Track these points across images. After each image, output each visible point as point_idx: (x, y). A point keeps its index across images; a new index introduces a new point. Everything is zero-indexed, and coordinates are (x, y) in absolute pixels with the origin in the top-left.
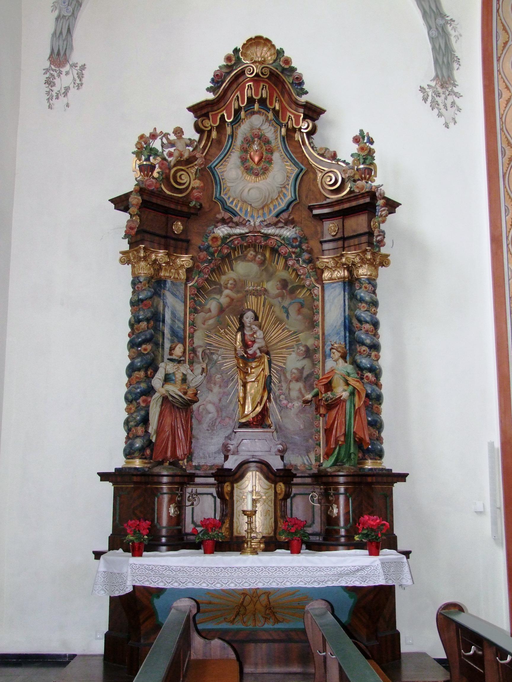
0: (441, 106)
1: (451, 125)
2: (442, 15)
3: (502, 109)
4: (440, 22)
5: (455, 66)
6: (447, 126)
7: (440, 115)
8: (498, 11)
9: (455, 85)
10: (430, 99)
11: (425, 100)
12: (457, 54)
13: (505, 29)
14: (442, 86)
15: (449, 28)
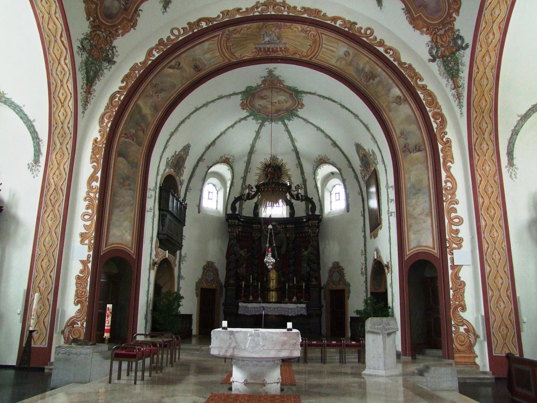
0: (34, 170)
1: (36, 177)
2: (39, 139)
3: (49, 171)
4: (38, 141)
5: (41, 156)
6: (34, 178)
7: (33, 173)
8: (53, 138)
9: (39, 163)
10: (30, 168)
11: (29, 168)
12: (42, 152)
13: (55, 144)
14: (35, 163)
15: (40, 142)
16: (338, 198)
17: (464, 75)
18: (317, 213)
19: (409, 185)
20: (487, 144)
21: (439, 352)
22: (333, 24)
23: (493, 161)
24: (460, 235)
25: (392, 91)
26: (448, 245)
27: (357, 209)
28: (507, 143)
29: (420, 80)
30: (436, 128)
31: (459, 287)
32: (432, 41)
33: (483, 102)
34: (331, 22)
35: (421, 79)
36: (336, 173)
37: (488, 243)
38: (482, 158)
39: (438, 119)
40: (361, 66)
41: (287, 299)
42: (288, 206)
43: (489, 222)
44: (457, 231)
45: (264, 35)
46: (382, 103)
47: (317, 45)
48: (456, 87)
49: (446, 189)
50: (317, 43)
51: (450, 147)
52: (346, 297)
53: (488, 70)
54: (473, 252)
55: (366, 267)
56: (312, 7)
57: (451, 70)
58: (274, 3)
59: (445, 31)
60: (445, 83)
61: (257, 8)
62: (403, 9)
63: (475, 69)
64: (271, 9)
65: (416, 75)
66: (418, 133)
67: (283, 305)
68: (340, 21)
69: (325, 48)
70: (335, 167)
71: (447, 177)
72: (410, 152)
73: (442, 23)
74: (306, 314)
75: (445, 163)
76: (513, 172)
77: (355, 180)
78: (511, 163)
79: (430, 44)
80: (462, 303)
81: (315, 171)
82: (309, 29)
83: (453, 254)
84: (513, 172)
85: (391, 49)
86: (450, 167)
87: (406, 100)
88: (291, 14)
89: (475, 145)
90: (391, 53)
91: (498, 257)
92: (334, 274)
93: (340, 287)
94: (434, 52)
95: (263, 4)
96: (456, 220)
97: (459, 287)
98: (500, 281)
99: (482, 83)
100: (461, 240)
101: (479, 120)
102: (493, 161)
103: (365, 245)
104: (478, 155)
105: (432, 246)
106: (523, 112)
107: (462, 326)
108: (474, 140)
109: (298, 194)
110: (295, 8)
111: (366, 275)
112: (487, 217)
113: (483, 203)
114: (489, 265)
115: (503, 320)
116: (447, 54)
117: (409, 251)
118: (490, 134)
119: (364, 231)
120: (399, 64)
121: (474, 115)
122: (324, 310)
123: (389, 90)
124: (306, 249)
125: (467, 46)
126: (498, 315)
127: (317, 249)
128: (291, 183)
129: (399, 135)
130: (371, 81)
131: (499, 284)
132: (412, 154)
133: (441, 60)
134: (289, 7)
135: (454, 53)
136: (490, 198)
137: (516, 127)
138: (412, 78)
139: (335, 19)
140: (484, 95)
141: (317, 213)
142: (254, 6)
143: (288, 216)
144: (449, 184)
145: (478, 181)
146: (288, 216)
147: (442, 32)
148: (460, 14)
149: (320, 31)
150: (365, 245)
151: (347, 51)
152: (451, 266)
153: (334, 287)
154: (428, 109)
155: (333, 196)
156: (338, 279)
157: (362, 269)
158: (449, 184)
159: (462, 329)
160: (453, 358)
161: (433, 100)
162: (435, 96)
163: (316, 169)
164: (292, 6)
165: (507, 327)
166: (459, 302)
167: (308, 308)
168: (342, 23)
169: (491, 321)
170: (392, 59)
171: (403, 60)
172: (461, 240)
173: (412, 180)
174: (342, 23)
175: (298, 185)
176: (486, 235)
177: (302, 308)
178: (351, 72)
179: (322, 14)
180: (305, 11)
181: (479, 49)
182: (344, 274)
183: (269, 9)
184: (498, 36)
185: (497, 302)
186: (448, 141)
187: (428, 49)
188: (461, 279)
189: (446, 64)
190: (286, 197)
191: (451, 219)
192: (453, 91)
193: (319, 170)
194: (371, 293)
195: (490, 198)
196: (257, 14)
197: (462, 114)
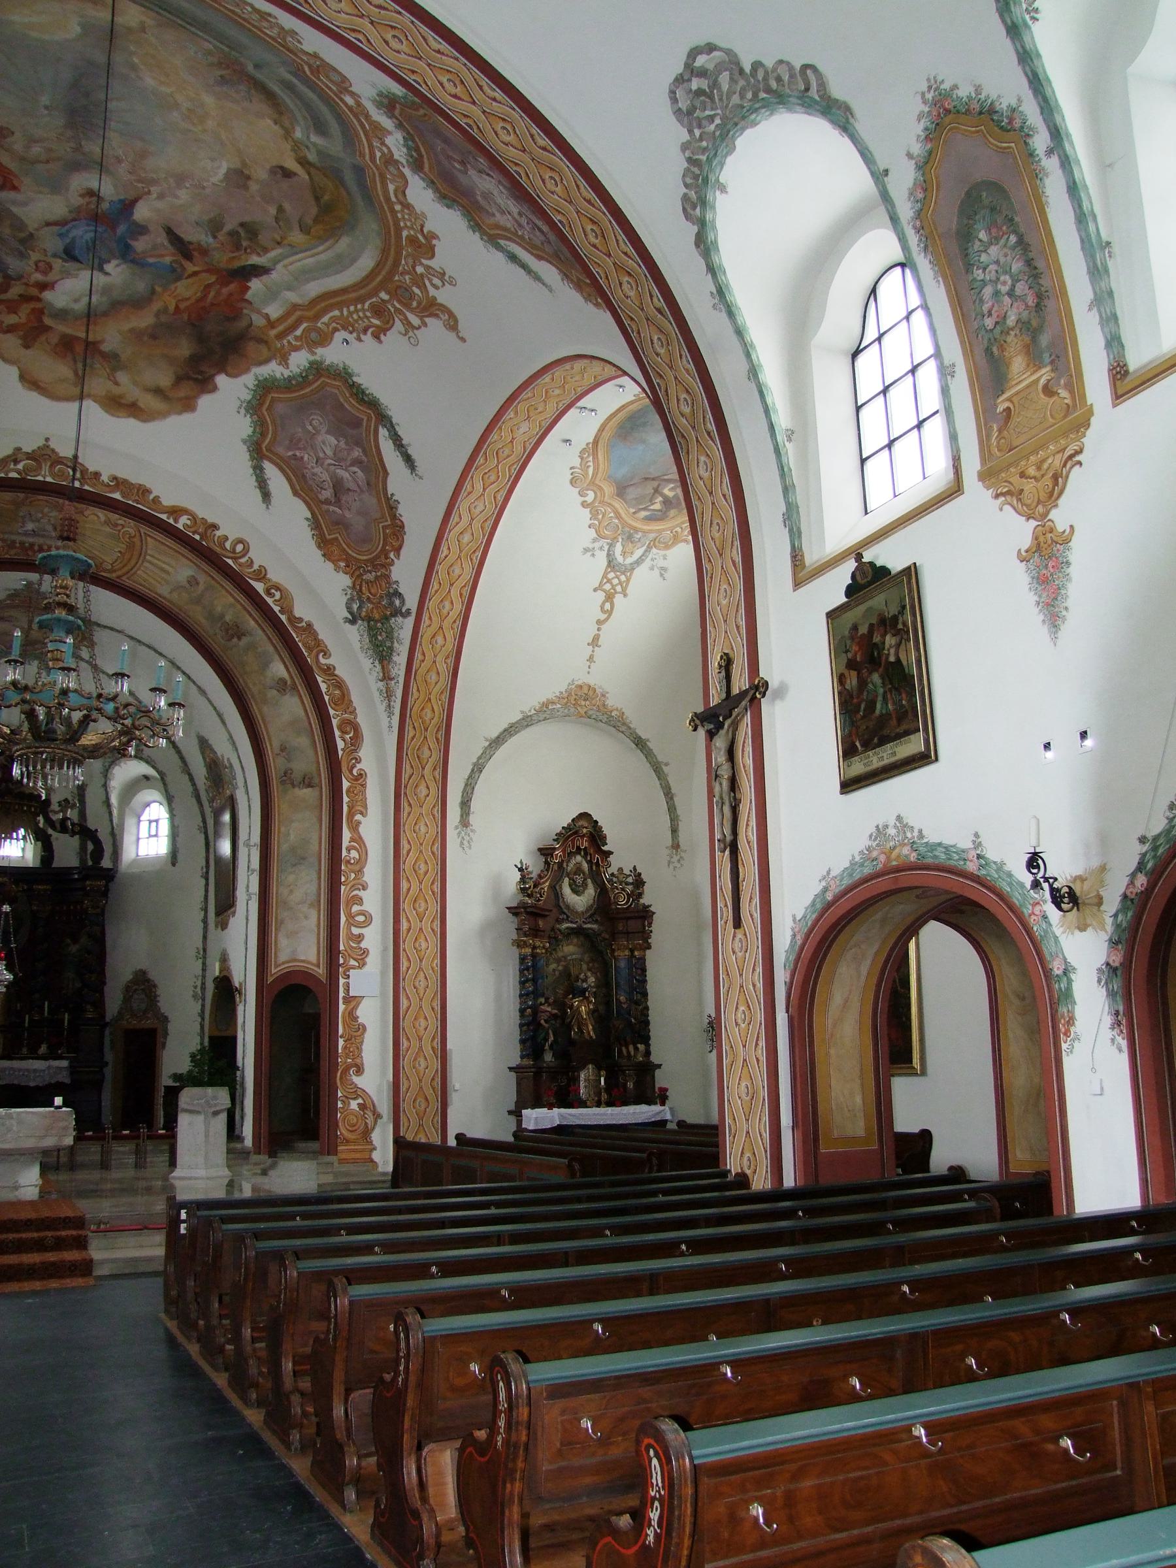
16: (153, 832)
17: (400, 660)
18: (106, 863)
19: (285, 847)
20: (428, 788)
21: (314, 1146)
22: (171, 521)
23: (433, 815)
24: (363, 945)
25: (271, 665)
26: (341, 961)
27: (195, 860)
28: (463, 785)
29: (325, 654)
30: (342, 750)
31: (356, 1034)
32: (354, 587)
33: (428, 711)
34: (168, 518)
35: (326, 654)
36: (153, 777)
37: (409, 960)
38: (416, 809)
39: (347, 733)
40: (219, 609)
41: (25, 1050)
42: (39, 843)
43: (415, 924)
44: (360, 938)
45: (23, 517)
46: (252, 686)
47: (136, 553)
48: (386, 677)
49: (348, 862)
50: (134, 551)
51: (364, 786)
52: (159, 1045)
53: (438, 659)
54: (383, 973)
55: (203, 984)
56: (133, 480)
57: (381, 645)
58: (53, 457)
59: (377, 577)
60: (368, 665)
61: (16, 462)
62: (307, 519)
63: (418, 656)
64: (45, 468)
65: (319, 646)
66: (310, 752)
67: (16, 1064)
68: (186, 517)
69: (150, 562)
70: (154, 767)
71: (352, 840)
72: (294, 786)
73: (372, 561)
74: (67, 1081)
75: (351, 815)
76: (467, 838)
77: (194, 801)
78: (465, 822)
79: (349, 592)
80: (358, 1061)
81: (107, 771)
82: (120, 522)
83: (348, 977)
84: (467, 838)
85: (278, 589)
86: (359, 823)
87: (294, 687)
88: (86, 487)
89: (406, 787)
90: (278, 595)
91: (423, 984)
92: (136, 996)
93: (148, 1023)
94: (355, 607)
95: (30, 456)
96: (361, 918)
97: (356, 1034)
98: (423, 1023)
99: (429, 680)
100: (366, 952)
101: (417, 742)
102: (433, 815)
103: (205, 937)
104: (410, 805)
105: (315, 961)
106: (494, 735)
107: (354, 1099)
108: (405, 777)
109: (65, 819)
110: (97, 475)
111: (203, 1000)
112: (412, 915)
113: (409, 890)
114: (408, 998)
115: (421, 1088)
116: (377, 616)
117: (276, 966)
118: (435, 769)
119: (206, 910)
120: (289, 619)
121: (409, 732)
122: (108, 1071)
123: (265, 665)
124: (75, 941)
125: (408, 612)
126: (414, 1081)
127: (100, 941)
128: (49, 790)
129: (277, 751)
130: (235, 640)
131: (422, 1029)
132: (296, 790)
133: (366, 624)
134: (84, 471)
135: (387, 618)
136: (421, 883)
137: (479, 758)
138: (310, 649)
139: (176, 512)
140: (430, 699)
141: (106, 863)
142: (8, 457)
143: (38, 864)
144: (354, 854)
145: (404, 852)
146: (38, 864)
147: (370, 577)
148: (401, 557)
149: (144, 529)
150: (205, 937)
151: (193, 576)
152: (344, 998)
153: (134, 1023)
154: (332, 712)
155: (144, 826)
156: (143, 1006)
157: (196, 987)
158: (354, 854)
159: (354, 1105)
160: (335, 1153)
161: (343, 695)
162: (348, 689)
163: (110, 766)
164: (91, 469)
165: (426, 1099)
166: (353, 1059)
167: (72, 1070)
168: (189, 522)
169: (403, 1089)
170: (276, 609)
171: (297, 613)
172: (366, 952)
173: (292, 837)
174: (189, 522)
175: (66, 800)
176: (407, 945)
177: (60, 1068)
178: (197, 617)
179: (151, 497)
180: (117, 485)
181: (427, 622)
182: (156, 996)
183: (41, 468)
184: (458, 607)
185: (415, 1059)
186: (361, 774)
187: (344, 599)
188: (360, 1020)
189: (372, 632)
190: (37, 823)
191: (350, 916)
192: (381, 684)
193: (117, 768)
194: (211, 1038)
195: (421, 883)
196: (14, 475)
197: (390, 727)
